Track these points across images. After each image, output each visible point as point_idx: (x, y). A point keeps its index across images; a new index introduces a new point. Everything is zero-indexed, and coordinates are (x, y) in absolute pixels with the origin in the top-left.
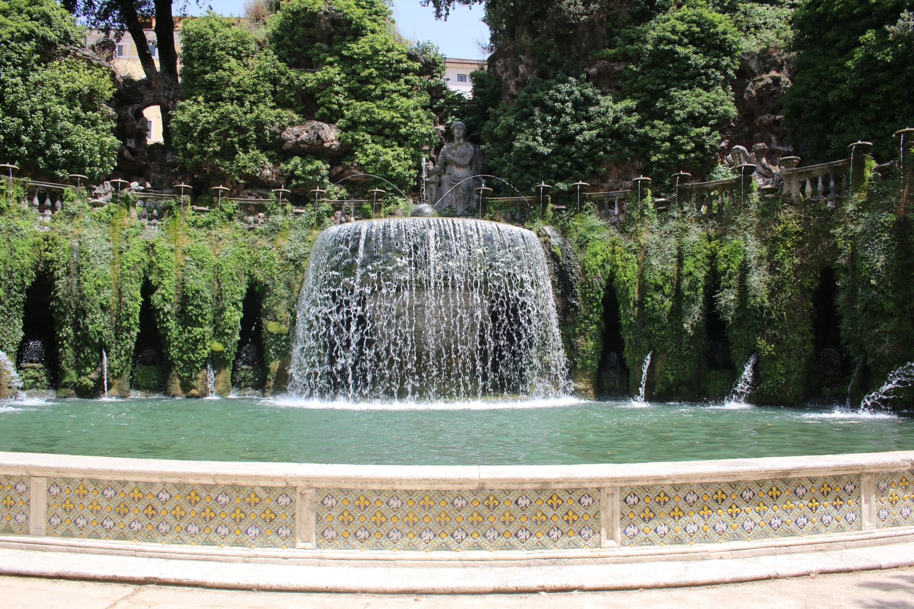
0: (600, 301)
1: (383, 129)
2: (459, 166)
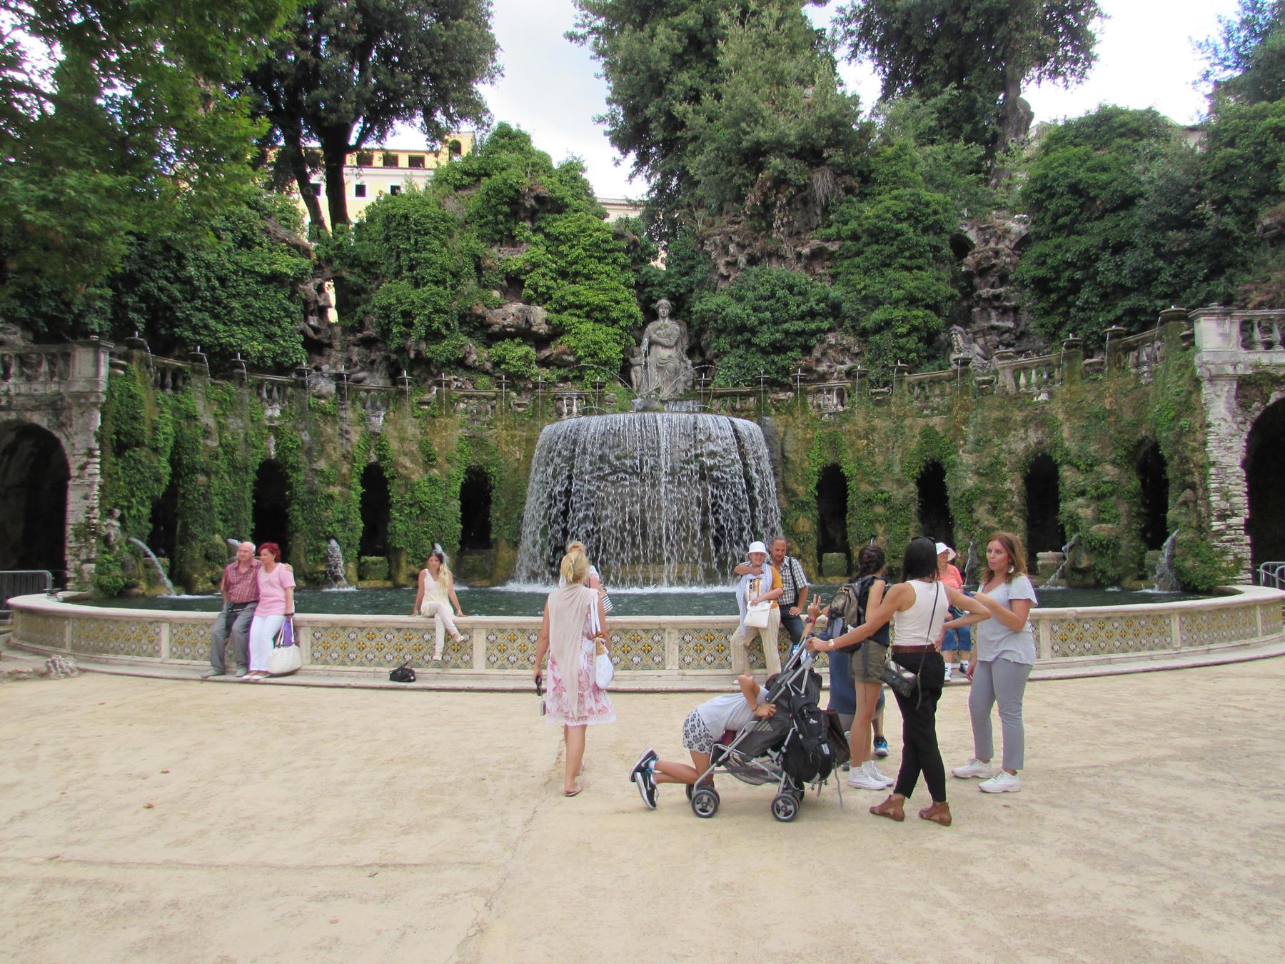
1: (592, 310)
2: (665, 347)
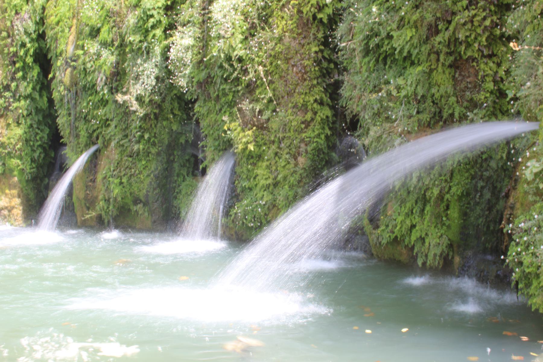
0: (29, 60)
